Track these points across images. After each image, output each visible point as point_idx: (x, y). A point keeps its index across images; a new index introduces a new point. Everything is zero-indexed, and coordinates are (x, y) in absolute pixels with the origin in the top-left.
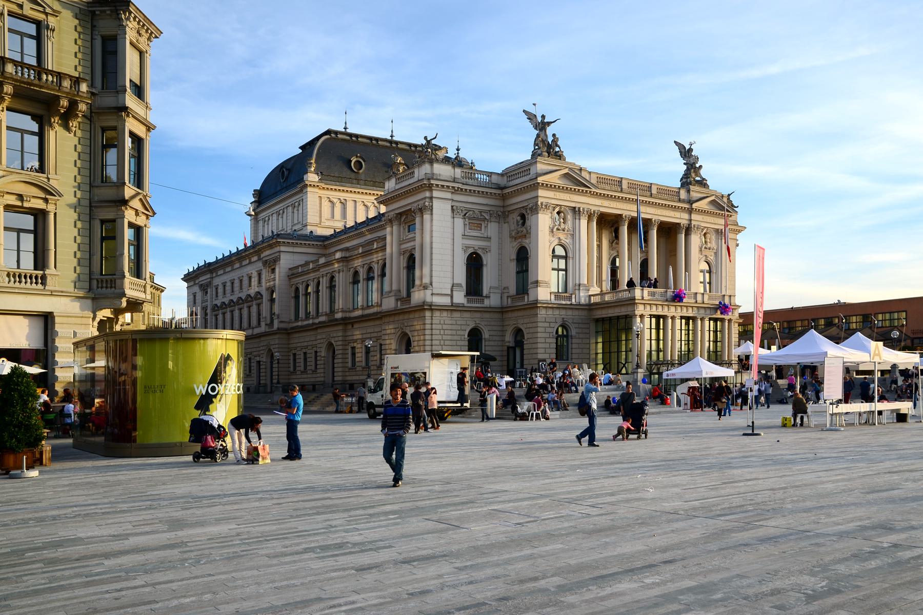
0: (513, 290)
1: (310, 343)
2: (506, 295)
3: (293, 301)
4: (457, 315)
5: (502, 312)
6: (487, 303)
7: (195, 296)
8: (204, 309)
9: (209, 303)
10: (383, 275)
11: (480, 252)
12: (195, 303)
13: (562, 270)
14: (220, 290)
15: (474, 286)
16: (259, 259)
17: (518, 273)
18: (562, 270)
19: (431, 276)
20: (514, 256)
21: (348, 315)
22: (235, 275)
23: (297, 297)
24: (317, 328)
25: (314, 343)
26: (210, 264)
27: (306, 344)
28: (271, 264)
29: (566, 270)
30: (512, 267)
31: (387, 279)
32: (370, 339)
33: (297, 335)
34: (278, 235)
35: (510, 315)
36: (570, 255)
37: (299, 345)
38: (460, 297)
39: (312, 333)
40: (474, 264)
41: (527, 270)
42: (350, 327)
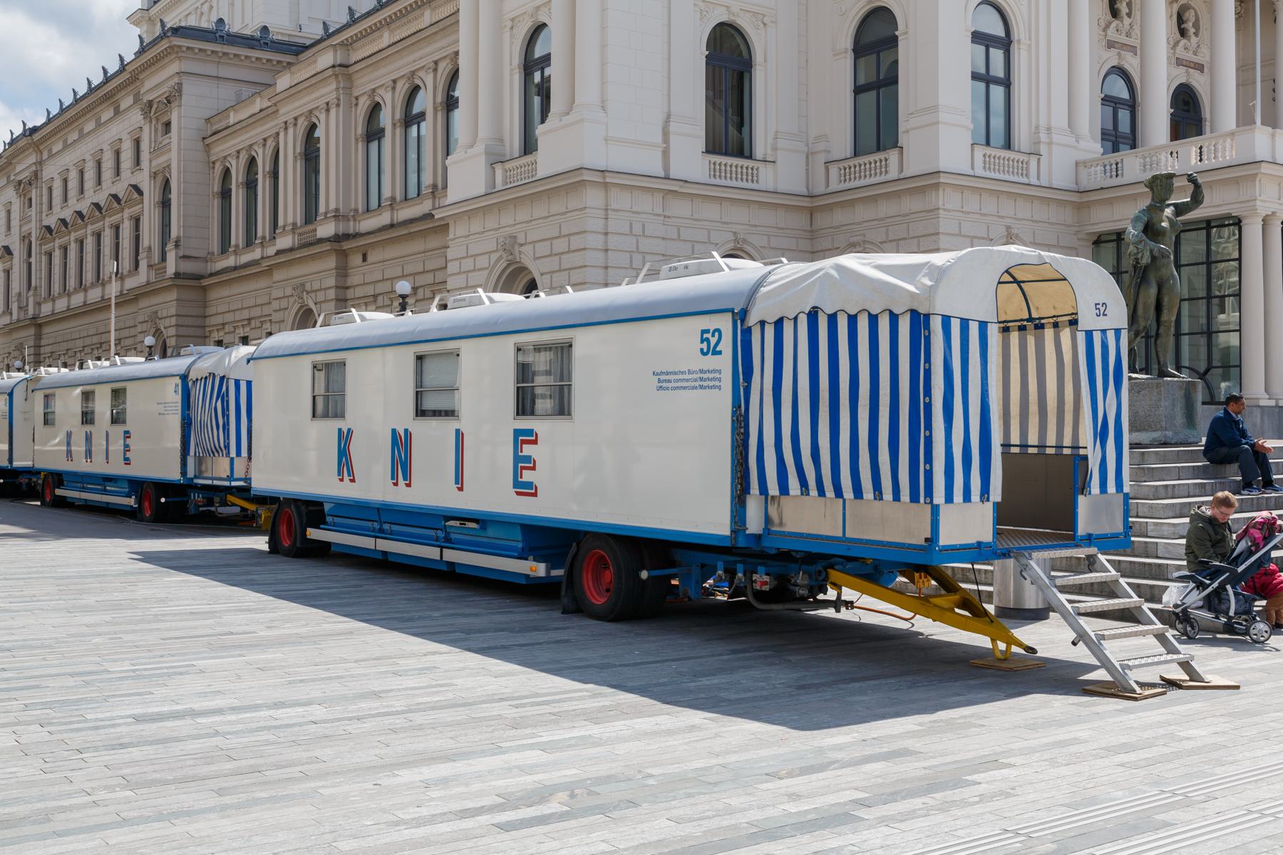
0: (842, 142)
1: (256, 312)
2: (821, 158)
3: (216, 203)
4: (680, 209)
5: (812, 212)
6: (767, 178)
7: (9, 212)
8: (26, 238)
9: (33, 224)
10: (450, 104)
11: (744, 23)
12: (9, 228)
13: (997, 81)
14: (57, 193)
15: (730, 126)
16: (137, 99)
17: (858, 90)
18: (997, 81)
19: (603, 83)
20: (847, 42)
21: (351, 228)
22: (85, 151)
23: (225, 194)
24: (269, 271)
25: (266, 310)
26: (34, 130)
27: (245, 314)
28: (159, 112)
29: (1007, 83)
30: (838, 74)
31: (458, 116)
32: (403, 277)
33: (225, 292)
34: (176, 31)
35: (839, 217)
36: (1019, 32)
37: (229, 317)
38: (691, 159)
39: (262, 283)
40: (729, 61)
41: (892, 80)
42: (356, 260)
